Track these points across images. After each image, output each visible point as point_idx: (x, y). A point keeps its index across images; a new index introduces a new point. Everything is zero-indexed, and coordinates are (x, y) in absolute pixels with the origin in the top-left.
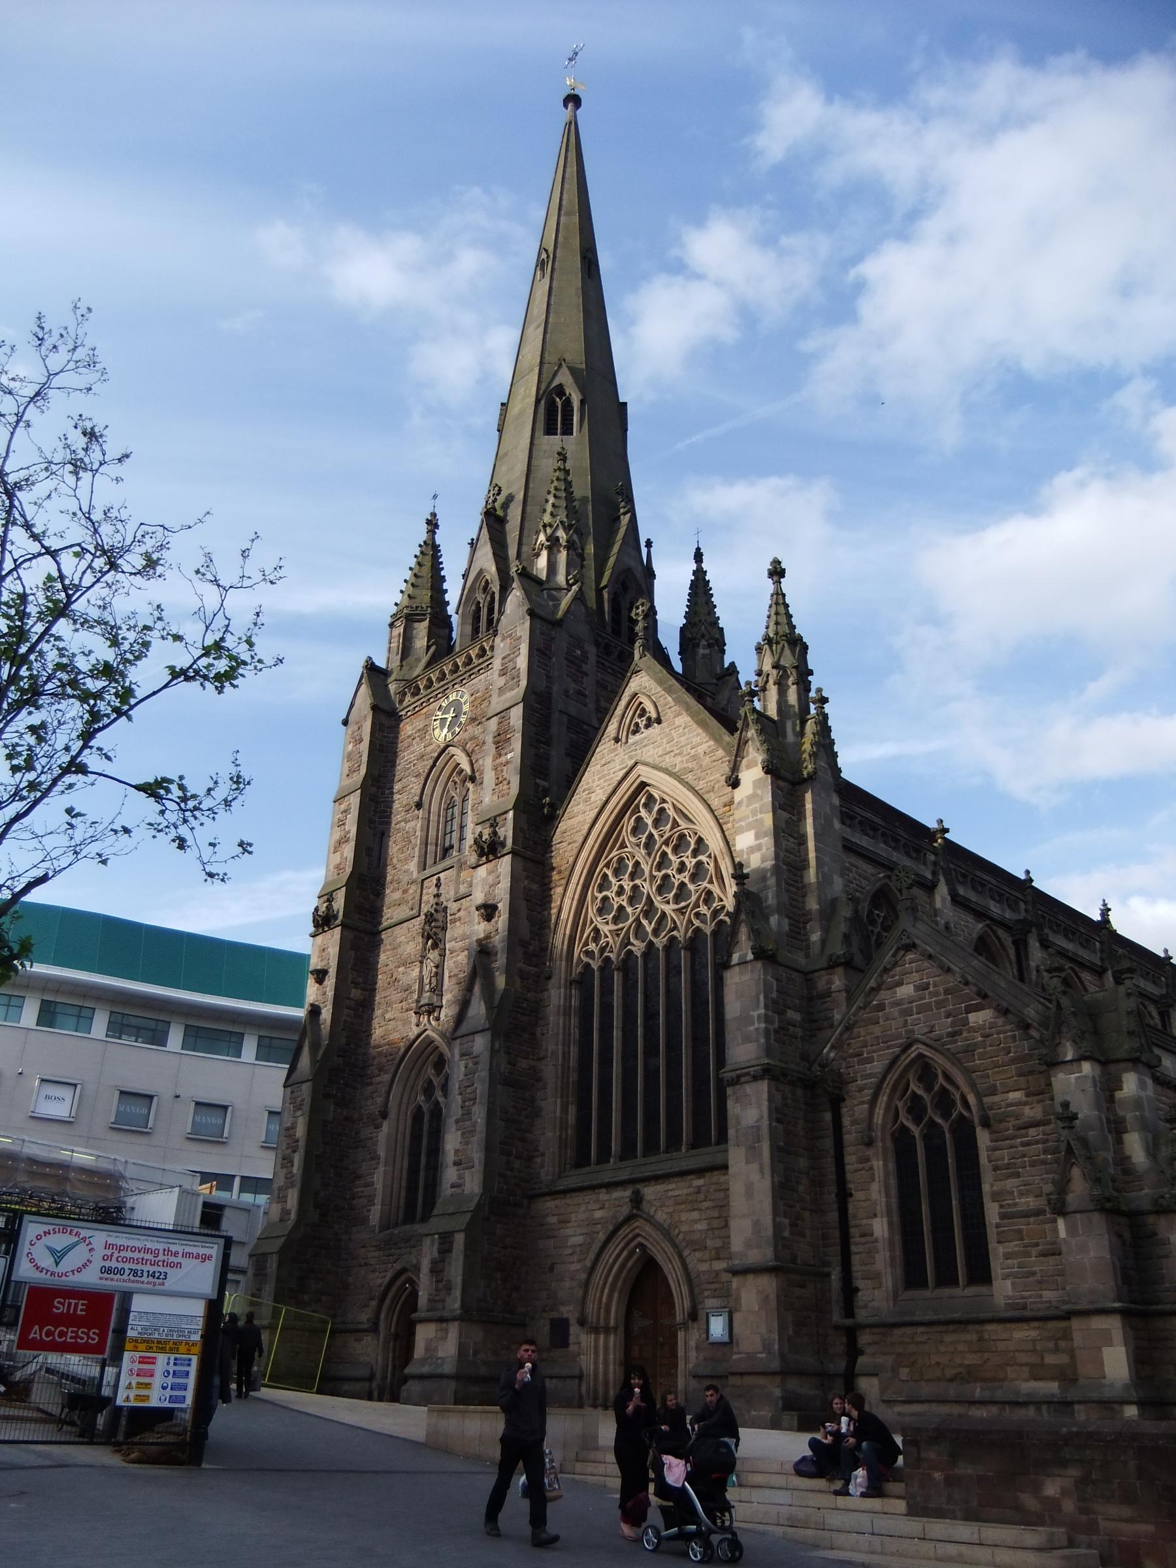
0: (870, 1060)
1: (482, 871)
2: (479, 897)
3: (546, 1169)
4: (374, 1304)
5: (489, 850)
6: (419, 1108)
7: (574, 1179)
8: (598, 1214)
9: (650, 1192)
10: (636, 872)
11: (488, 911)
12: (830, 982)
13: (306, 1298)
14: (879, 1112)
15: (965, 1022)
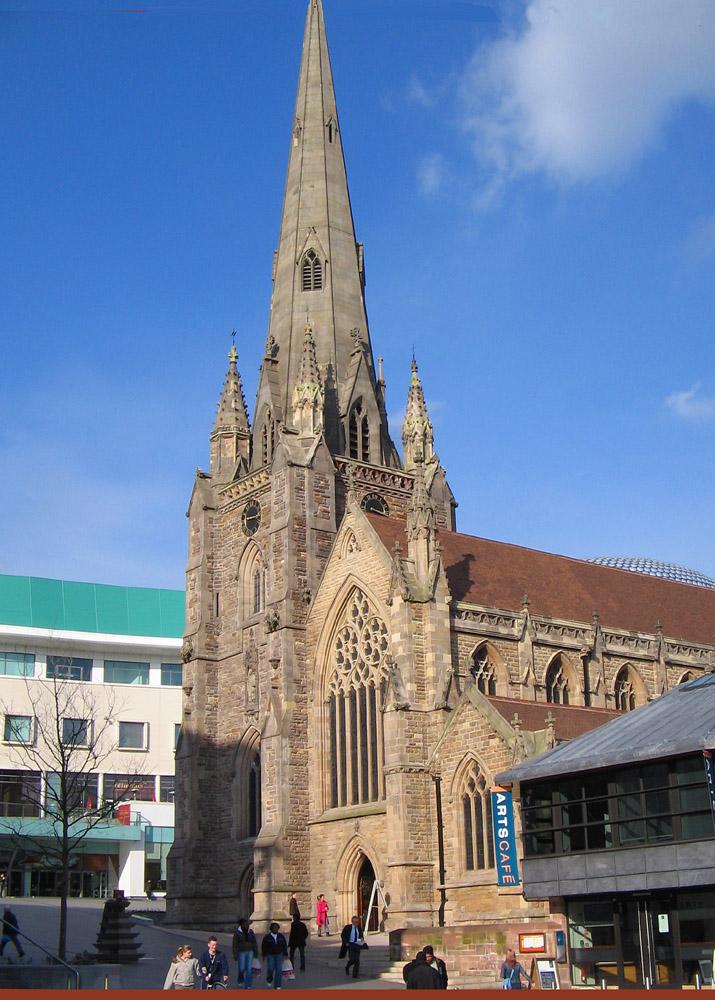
0: (451, 760)
1: (272, 635)
2: (270, 652)
3: (315, 809)
4: (238, 882)
5: (274, 626)
6: (253, 770)
7: (332, 813)
8: (341, 834)
9: (364, 822)
10: (355, 641)
11: (275, 663)
12: (436, 718)
13: (201, 880)
14: (455, 786)
15: (488, 744)
